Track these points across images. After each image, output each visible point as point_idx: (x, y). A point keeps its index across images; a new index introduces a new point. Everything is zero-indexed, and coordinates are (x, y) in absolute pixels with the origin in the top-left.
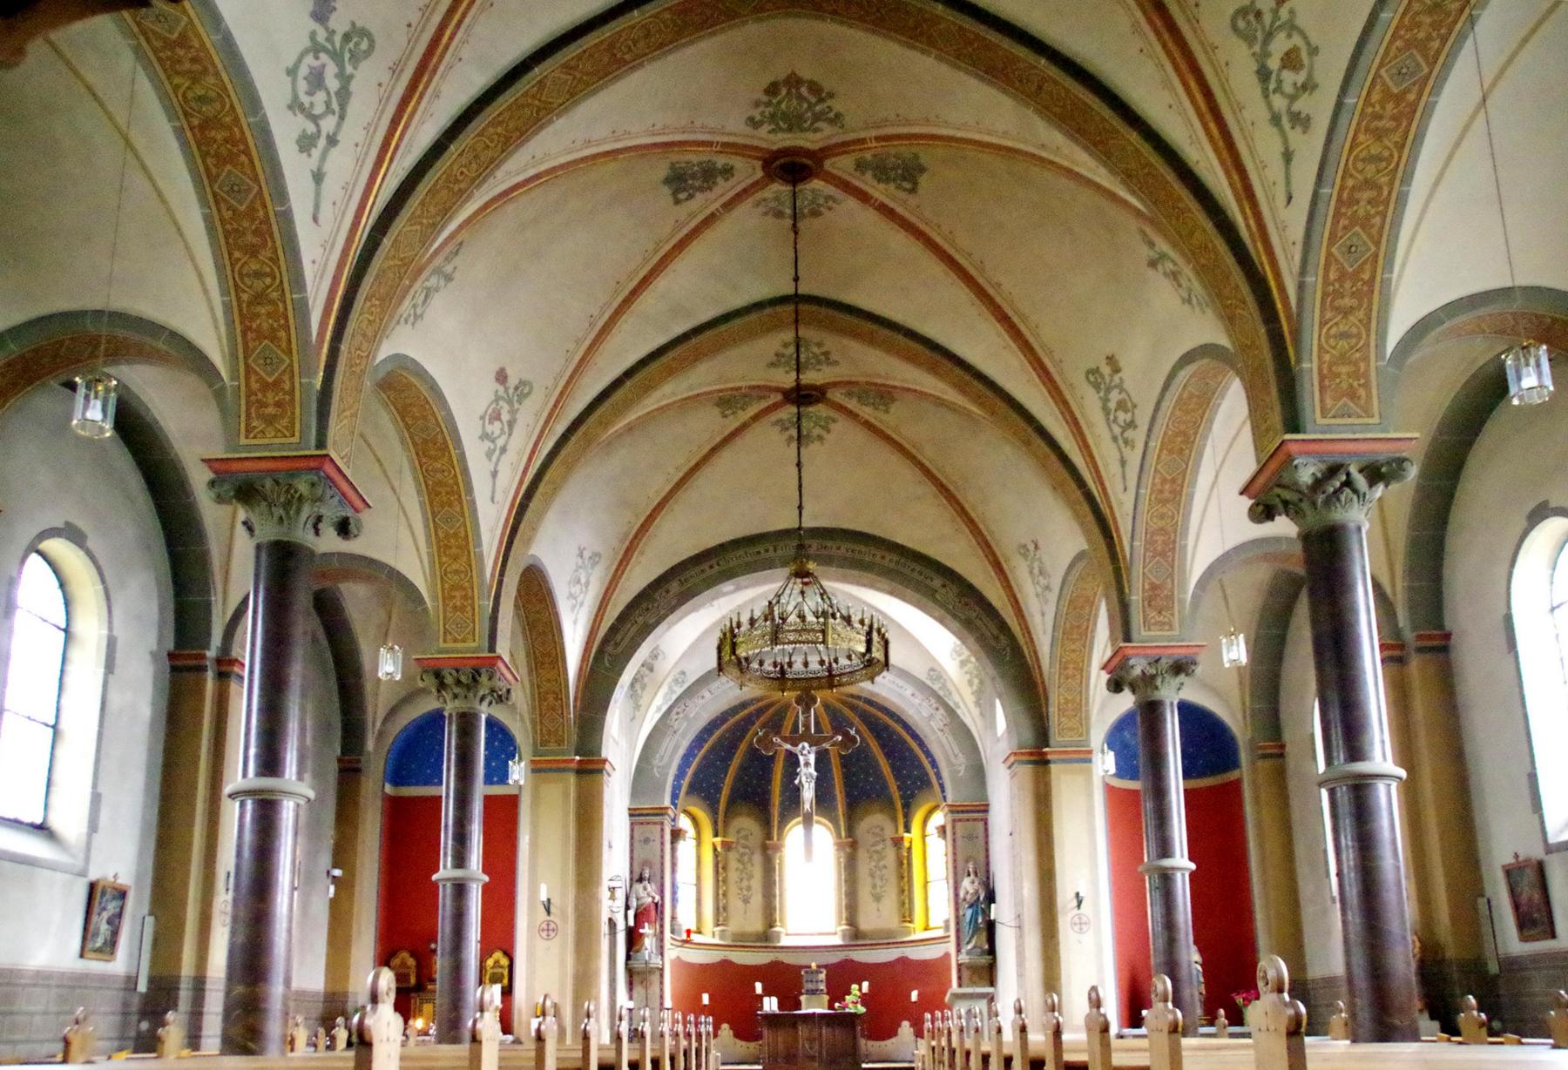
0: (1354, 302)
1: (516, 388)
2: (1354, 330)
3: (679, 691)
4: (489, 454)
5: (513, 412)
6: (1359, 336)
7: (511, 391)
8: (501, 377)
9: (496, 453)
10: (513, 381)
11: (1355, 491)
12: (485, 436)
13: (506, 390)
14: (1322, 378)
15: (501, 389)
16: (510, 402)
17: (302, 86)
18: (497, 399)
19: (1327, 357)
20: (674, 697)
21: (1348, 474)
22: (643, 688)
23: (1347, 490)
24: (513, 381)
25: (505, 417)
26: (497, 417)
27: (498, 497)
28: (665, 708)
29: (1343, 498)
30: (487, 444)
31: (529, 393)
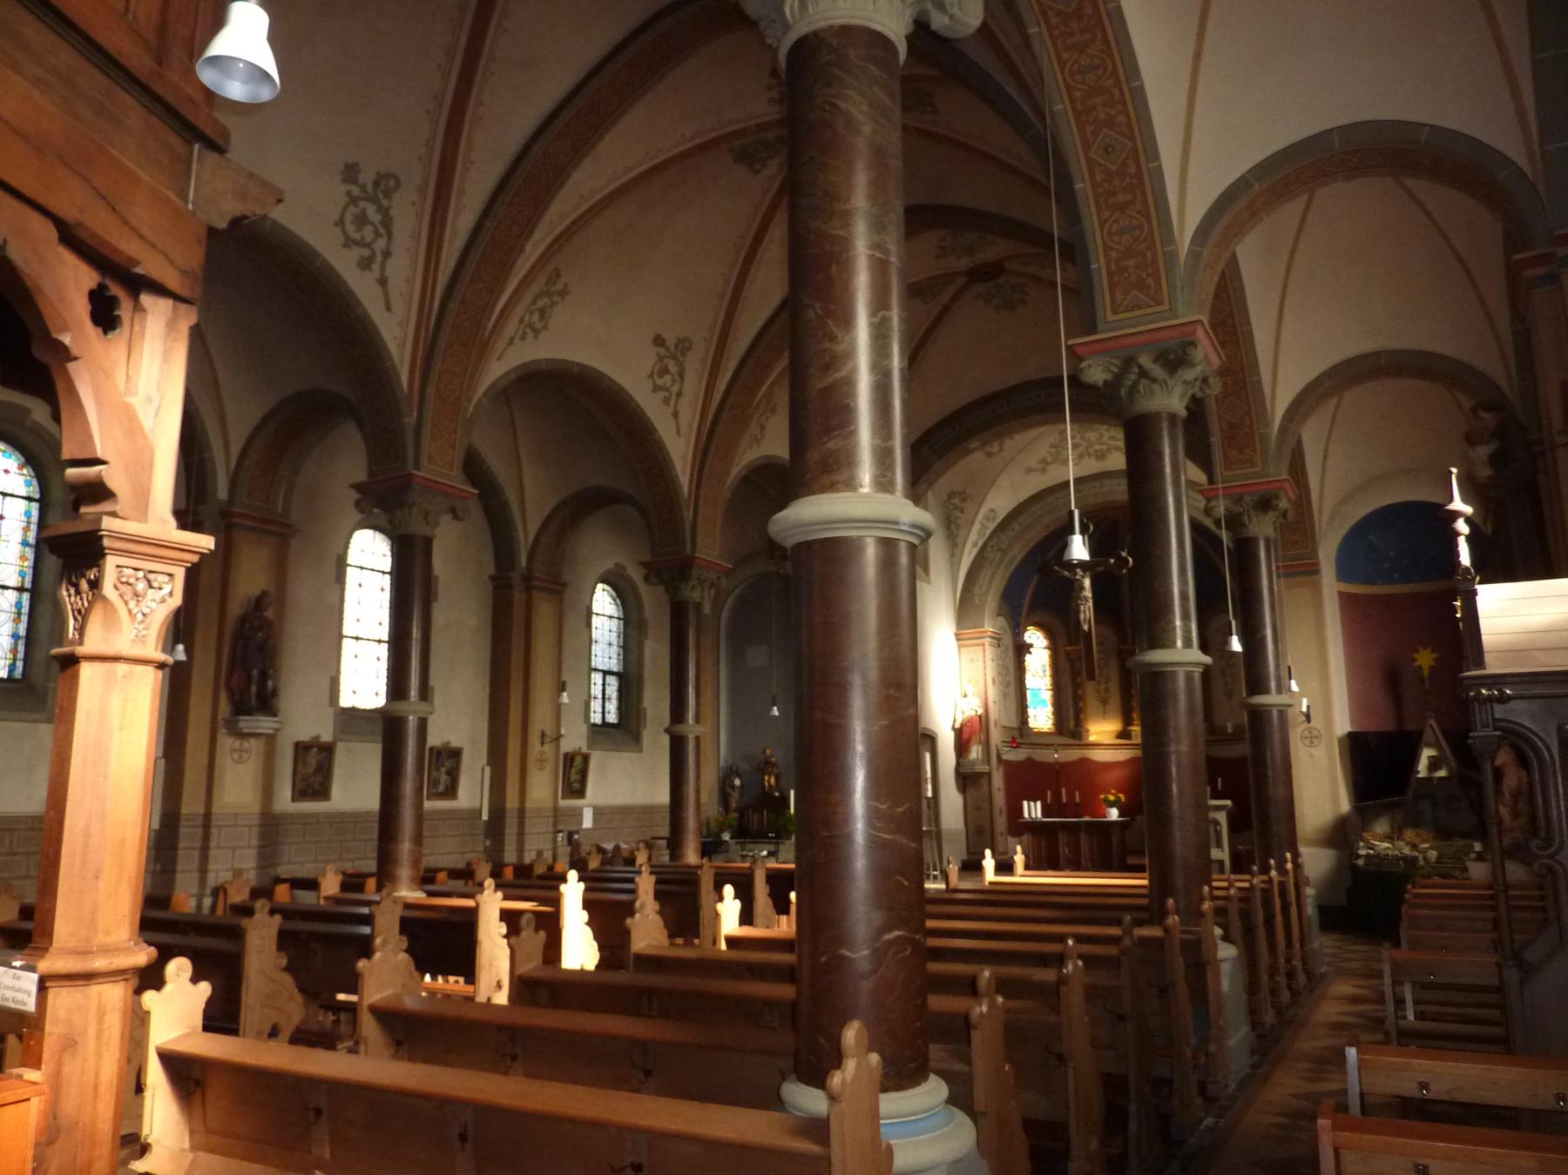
0: (1128, 197)
2: (1135, 222)
3: (992, 526)
4: (666, 401)
5: (680, 365)
6: (1141, 227)
8: (659, 341)
9: (672, 400)
10: (671, 340)
11: (1154, 380)
12: (656, 388)
13: (668, 350)
14: (1110, 275)
15: (662, 351)
16: (674, 357)
17: (351, 229)
18: (660, 358)
19: (1114, 254)
20: (988, 533)
21: (1140, 366)
22: (958, 528)
23: (1143, 381)
25: (672, 367)
26: (664, 371)
27: (684, 429)
28: (980, 544)
29: (1141, 388)
30: (662, 394)
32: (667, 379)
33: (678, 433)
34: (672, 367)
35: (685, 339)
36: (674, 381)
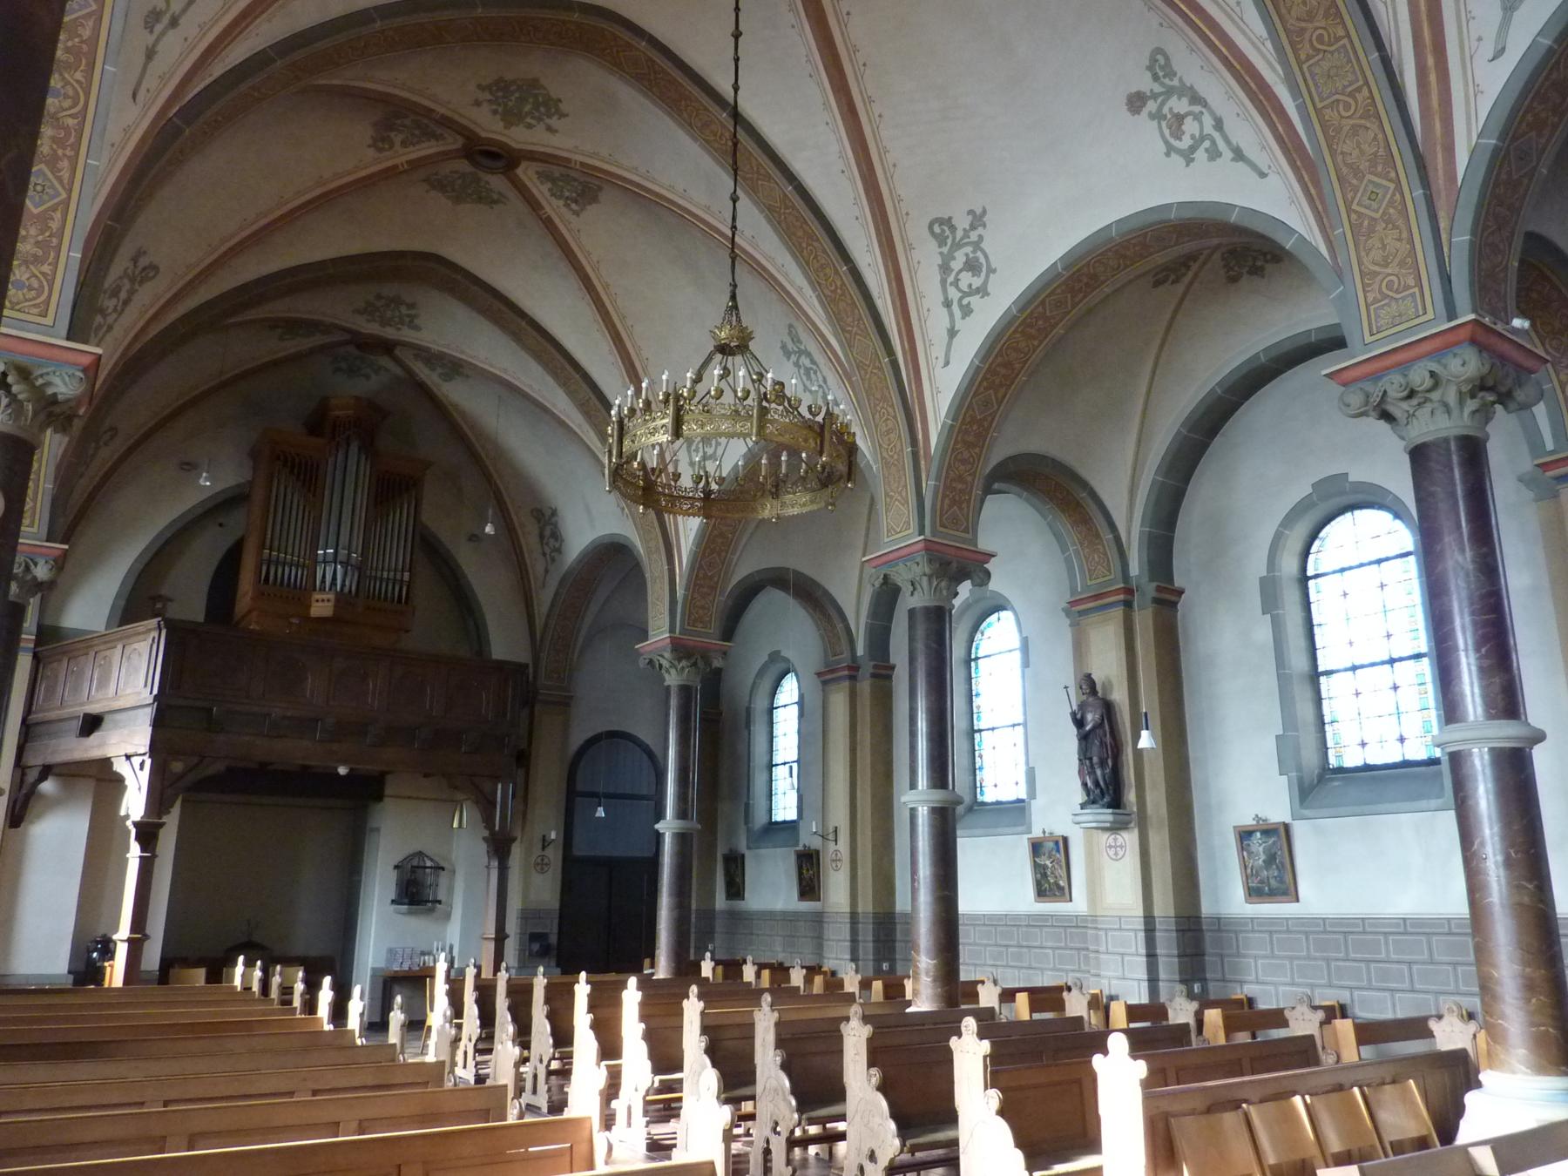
1: (1156, 78)
7: (1157, 88)
8: (1136, 102)
10: (1145, 84)
12: (1188, 156)
13: (1154, 96)
15: (1151, 106)
16: (1170, 91)
18: (1157, 116)
24: (1145, 84)
30: (1200, 155)
31: (1167, 59)
32: (1190, 127)
33: (1263, 175)
34: (1180, 105)
35: (1153, 60)
36: (1198, 117)
